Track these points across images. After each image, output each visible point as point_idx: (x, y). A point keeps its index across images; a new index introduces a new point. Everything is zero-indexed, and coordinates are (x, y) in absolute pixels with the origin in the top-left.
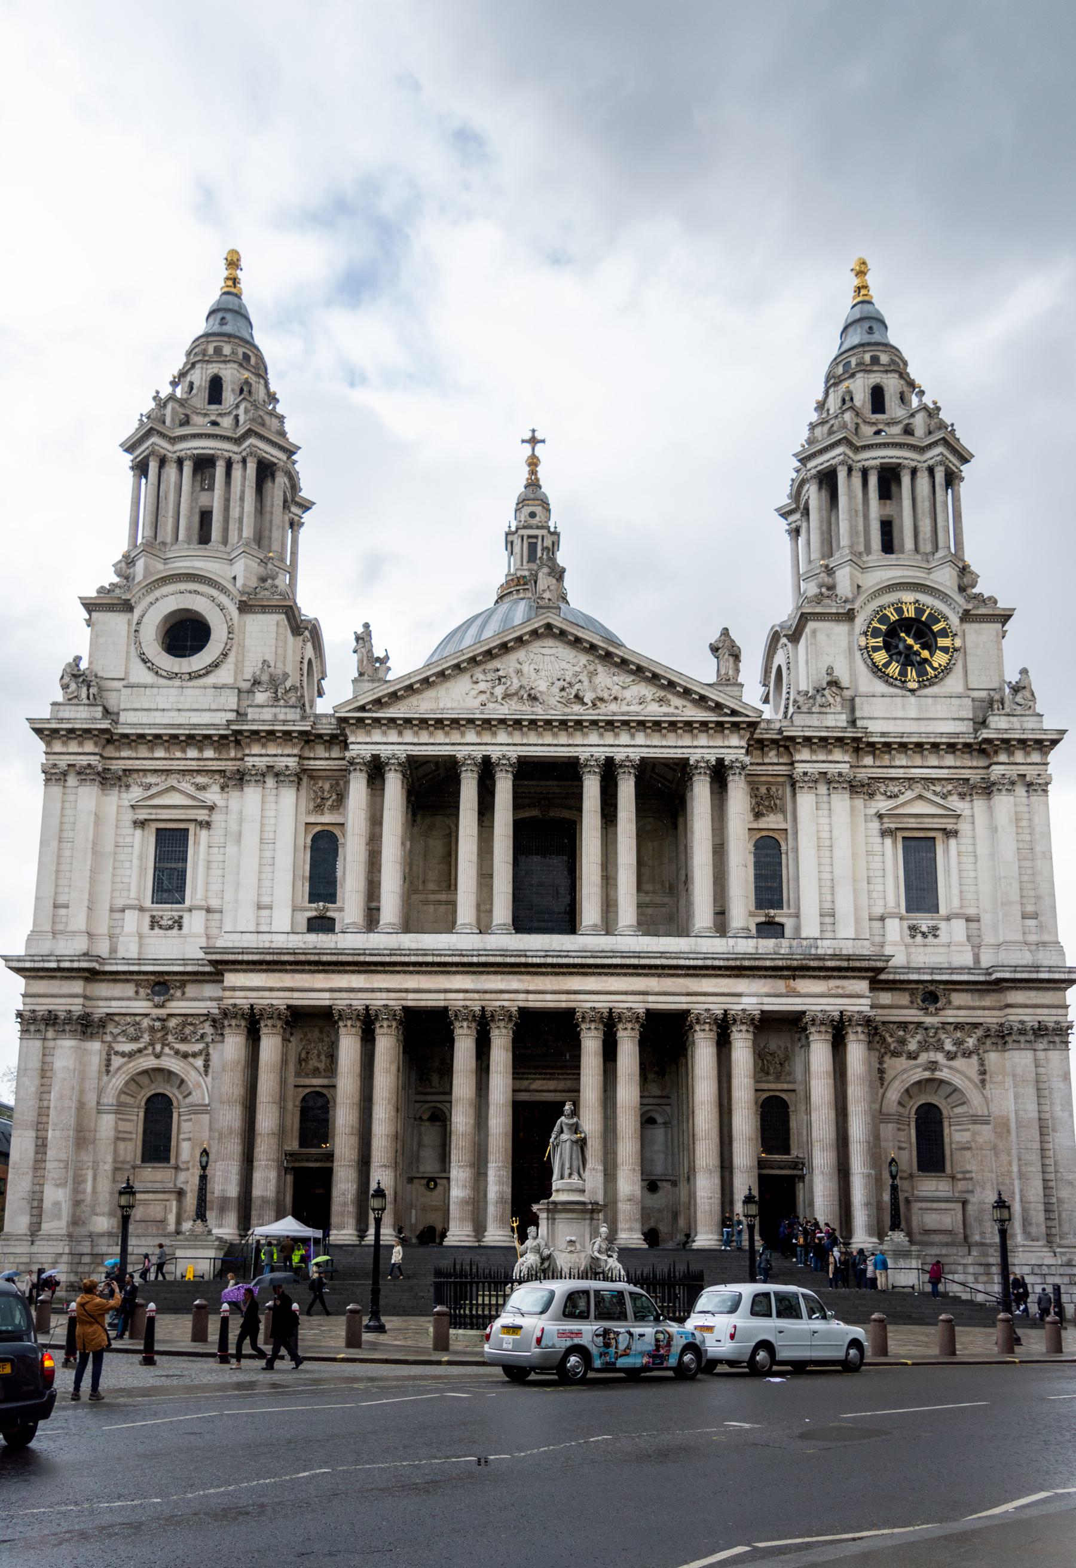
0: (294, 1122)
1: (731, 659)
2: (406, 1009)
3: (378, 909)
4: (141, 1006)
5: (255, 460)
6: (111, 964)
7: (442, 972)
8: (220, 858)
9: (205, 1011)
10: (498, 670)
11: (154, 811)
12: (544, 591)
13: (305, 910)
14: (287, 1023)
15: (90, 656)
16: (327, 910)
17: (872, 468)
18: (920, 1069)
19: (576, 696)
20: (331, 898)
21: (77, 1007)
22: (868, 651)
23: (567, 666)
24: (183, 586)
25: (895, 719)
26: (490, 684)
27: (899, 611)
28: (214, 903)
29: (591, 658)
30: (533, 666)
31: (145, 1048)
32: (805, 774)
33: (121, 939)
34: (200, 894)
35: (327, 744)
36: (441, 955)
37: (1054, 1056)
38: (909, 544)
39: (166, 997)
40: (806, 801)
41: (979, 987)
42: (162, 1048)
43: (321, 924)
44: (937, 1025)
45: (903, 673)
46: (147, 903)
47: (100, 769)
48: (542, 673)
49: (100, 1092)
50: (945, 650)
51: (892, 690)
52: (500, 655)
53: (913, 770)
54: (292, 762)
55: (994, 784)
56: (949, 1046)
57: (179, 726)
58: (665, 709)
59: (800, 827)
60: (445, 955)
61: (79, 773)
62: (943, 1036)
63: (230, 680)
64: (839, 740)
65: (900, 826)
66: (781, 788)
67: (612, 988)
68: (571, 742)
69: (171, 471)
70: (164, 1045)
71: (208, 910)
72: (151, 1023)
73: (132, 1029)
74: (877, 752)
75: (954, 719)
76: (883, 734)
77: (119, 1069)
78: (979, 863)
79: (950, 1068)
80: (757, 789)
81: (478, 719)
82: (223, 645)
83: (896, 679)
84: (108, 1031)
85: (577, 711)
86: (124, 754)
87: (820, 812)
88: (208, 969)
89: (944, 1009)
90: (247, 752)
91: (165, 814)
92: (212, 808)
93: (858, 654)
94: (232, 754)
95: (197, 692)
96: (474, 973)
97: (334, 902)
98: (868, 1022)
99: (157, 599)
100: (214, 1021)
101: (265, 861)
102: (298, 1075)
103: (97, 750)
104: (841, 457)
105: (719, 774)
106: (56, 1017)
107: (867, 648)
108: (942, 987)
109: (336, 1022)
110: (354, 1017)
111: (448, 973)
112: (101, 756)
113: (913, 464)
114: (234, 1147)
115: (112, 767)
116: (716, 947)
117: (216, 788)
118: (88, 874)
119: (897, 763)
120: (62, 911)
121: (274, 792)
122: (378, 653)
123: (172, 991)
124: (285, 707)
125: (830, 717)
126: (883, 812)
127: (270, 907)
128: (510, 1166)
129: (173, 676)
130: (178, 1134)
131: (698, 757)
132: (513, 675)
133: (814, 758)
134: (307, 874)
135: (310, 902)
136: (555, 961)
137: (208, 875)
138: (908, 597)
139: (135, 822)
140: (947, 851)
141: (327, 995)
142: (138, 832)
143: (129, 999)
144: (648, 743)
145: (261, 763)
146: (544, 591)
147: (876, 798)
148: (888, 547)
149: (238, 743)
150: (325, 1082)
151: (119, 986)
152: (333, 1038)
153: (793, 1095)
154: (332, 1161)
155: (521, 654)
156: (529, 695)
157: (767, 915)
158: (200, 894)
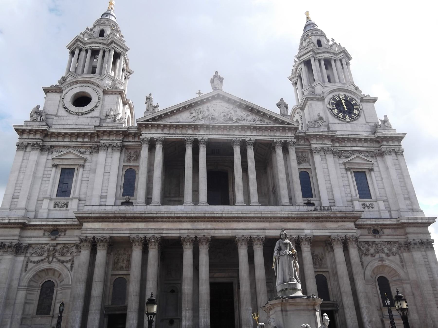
0: (110, 292)
1: (285, 108)
2: (162, 237)
3: (151, 198)
6: (34, 221)
7: (178, 222)
8: (87, 179)
9: (74, 242)
10: (200, 109)
11: (61, 161)
12: (216, 85)
17: (322, 59)
18: (377, 261)
19: (230, 118)
20: (133, 195)
21: (15, 240)
22: (331, 110)
23: (226, 109)
25: (344, 131)
28: (82, 197)
29: (235, 106)
30: (213, 108)
31: (45, 259)
32: (316, 148)
33: (40, 211)
34: (77, 193)
36: (178, 214)
37: (429, 253)
38: (337, 80)
39: (57, 236)
40: (317, 158)
41: (394, 227)
42: (53, 259)
43: (127, 203)
44: (381, 243)
46: (54, 196)
47: (41, 144)
49: (20, 280)
50: (357, 109)
51: (341, 122)
53: (354, 148)
54: (119, 143)
55: (384, 152)
56: (386, 251)
58: (262, 123)
60: (180, 214)
61: (32, 146)
62: (384, 247)
64: (326, 136)
65: (352, 167)
66: (306, 154)
68: (228, 134)
69: (83, 54)
71: (80, 200)
72: (49, 248)
74: (340, 141)
75: (365, 131)
76: (342, 135)
77: (31, 269)
79: (389, 260)
80: (298, 154)
81: (193, 125)
83: (342, 118)
84: (28, 252)
86: (52, 140)
88: (76, 223)
89: (382, 236)
90: (102, 139)
91: (66, 162)
92: (85, 160)
93: (327, 111)
95: (84, 119)
96: (192, 222)
97: (133, 196)
98: (356, 239)
99: (73, 88)
100: (77, 246)
101: (105, 180)
102: (113, 270)
103: (41, 138)
104: (311, 55)
105: (285, 147)
106: (5, 245)
107: (330, 108)
108: (380, 227)
109: (132, 244)
110: (139, 241)
111: (181, 222)
112: (42, 140)
113: (335, 58)
114: (80, 303)
116: (292, 211)
117: (88, 153)
118: (29, 184)
119: (347, 145)
120: (16, 200)
121: (111, 153)
122: (154, 104)
123: (60, 233)
127: (106, 197)
128: (209, 309)
129: (75, 114)
130: (55, 300)
131: (277, 140)
132: (206, 110)
133: (318, 143)
134: (122, 185)
135: (123, 196)
136: (226, 215)
137: (81, 186)
138: (342, 93)
139: (53, 165)
140: (371, 176)
141: (128, 232)
142: (54, 169)
143: (40, 237)
144: (258, 134)
145: (107, 143)
146: (216, 85)
147: (342, 158)
148: (329, 81)
149: (98, 136)
150: (125, 272)
152: (130, 253)
153: (327, 273)
154: (127, 310)
155: (208, 104)
156: (212, 118)
157: (307, 200)
158: (77, 193)
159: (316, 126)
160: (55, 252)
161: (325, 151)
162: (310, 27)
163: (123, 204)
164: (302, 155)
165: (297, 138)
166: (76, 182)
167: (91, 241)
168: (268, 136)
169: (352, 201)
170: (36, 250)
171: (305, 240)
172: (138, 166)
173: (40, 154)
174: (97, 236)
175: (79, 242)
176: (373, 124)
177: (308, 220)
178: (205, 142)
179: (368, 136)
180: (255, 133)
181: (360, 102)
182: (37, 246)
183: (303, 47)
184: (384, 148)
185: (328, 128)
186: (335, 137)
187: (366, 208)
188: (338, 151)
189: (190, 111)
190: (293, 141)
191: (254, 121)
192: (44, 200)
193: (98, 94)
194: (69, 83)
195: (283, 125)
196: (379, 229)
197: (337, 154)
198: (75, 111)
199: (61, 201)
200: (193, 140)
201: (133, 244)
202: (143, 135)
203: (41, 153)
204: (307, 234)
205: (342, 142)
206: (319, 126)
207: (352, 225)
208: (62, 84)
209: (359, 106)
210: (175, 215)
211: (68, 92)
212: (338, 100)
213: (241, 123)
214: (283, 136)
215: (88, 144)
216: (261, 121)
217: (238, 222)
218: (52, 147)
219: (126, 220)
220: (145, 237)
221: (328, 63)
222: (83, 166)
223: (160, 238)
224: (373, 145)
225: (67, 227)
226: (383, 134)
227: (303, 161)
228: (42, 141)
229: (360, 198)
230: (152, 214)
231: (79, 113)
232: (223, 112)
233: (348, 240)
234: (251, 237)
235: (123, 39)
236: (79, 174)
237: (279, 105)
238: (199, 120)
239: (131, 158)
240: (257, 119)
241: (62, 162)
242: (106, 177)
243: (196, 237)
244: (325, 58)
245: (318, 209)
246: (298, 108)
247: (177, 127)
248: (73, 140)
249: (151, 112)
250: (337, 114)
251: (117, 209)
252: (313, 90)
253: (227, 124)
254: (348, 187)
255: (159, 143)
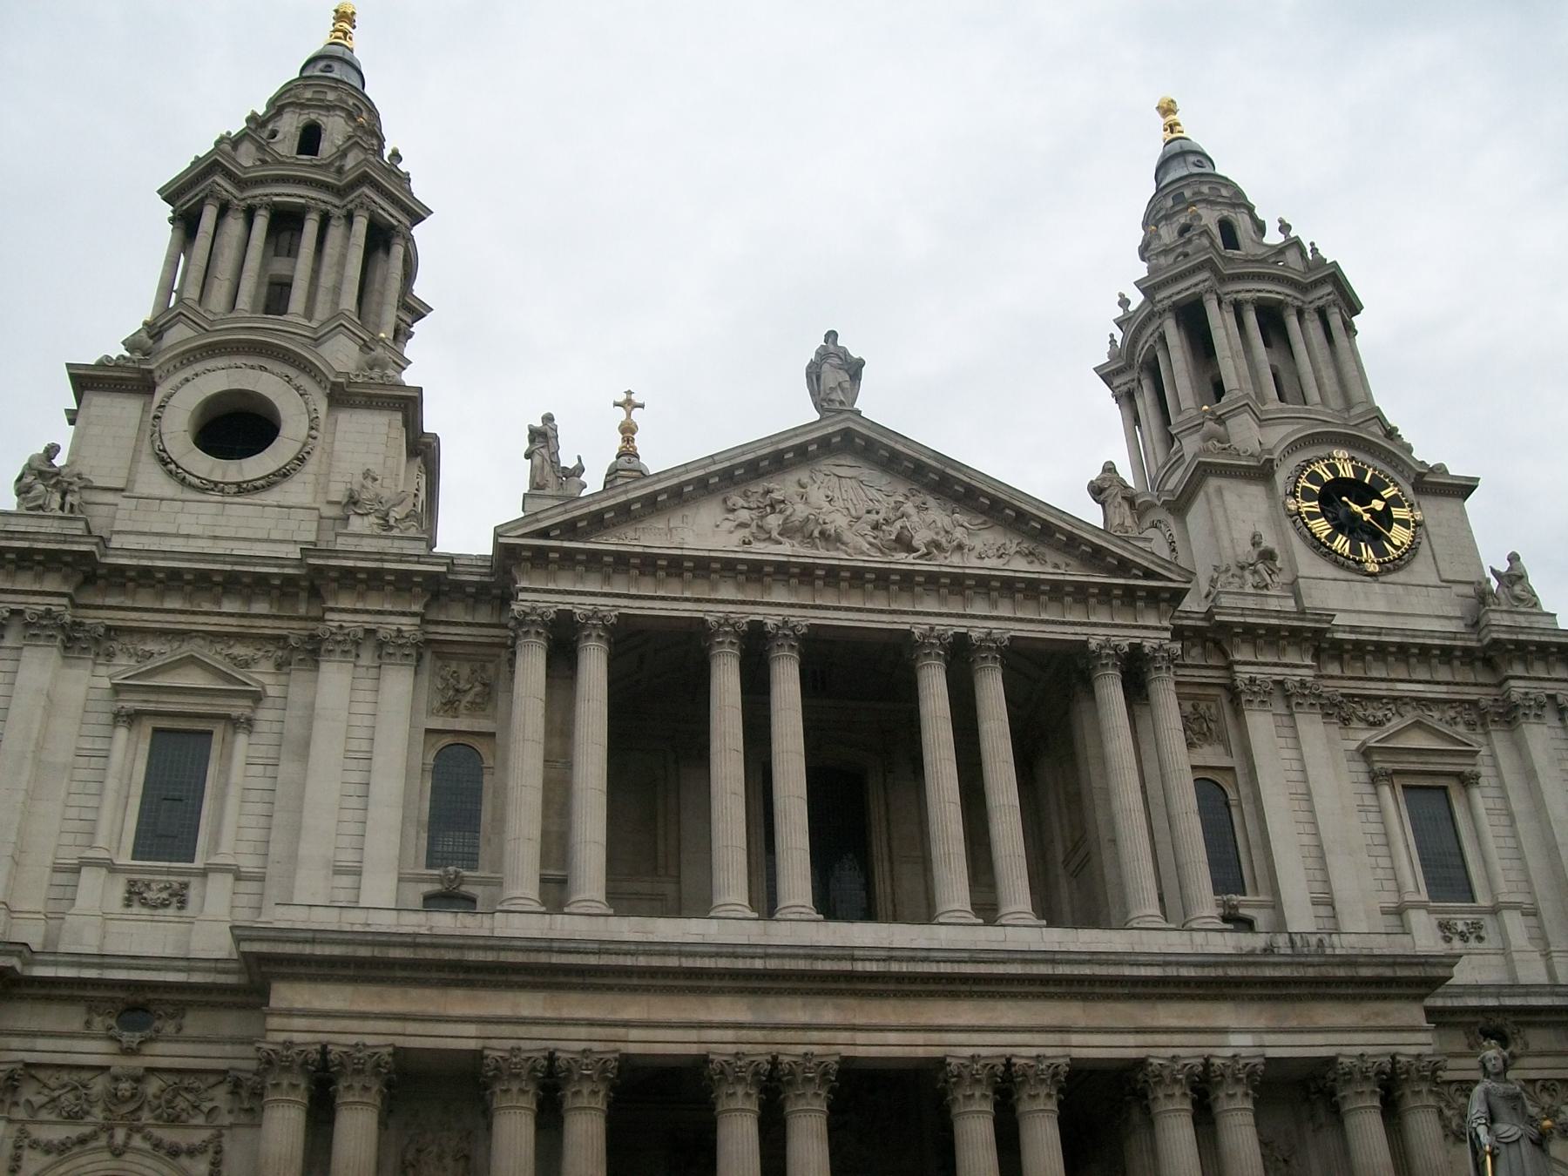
1: (1126, 506)
2: (625, 1059)
4: (93, 1051)
5: (367, 216)
6: (45, 964)
8: (267, 784)
10: (769, 492)
11: (153, 697)
13: (420, 879)
14: (389, 1085)
15: (71, 454)
16: (461, 880)
19: (899, 539)
20: (472, 861)
24: (239, 361)
25: (1359, 612)
26: (755, 514)
27: (1333, 468)
28: (248, 863)
32: (1252, 681)
35: (471, 601)
38: (1313, 395)
39: (148, 1033)
40: (1261, 725)
42: (129, 1137)
45: (1355, 550)
48: (839, 504)
50: (1404, 523)
51: (1342, 574)
52: (768, 473)
55: (1517, 706)
57: (214, 557)
58: (1036, 567)
59: (1259, 760)
60: (703, 955)
63: (307, 500)
65: (1397, 767)
67: (1005, 1022)
69: (235, 226)
70: (132, 1130)
71: (239, 876)
73: (71, 1096)
74: (1346, 657)
76: (1353, 629)
78: (1519, 825)
82: (299, 446)
85: (903, 560)
86: (110, 601)
87: (1282, 742)
90: (331, 604)
92: (257, 697)
93: (1288, 523)
94: (302, 611)
97: (474, 868)
99: (197, 375)
100: (237, 1085)
103: (65, 589)
108: (1513, 1019)
113: (1300, 304)
115: (88, 621)
117: (267, 666)
119: (1374, 674)
121: (373, 672)
124: (402, 538)
125: (1269, 599)
126: (1372, 744)
134: (425, 817)
136: (905, 968)
138: (1341, 453)
141: (471, 1029)
142: (122, 734)
143: (71, 1035)
151: (55, 1009)
155: (803, 475)
156: (822, 533)
159: (1249, 589)
160: (139, 1108)
161: (1289, 697)
162: (1183, 164)
163: (433, 902)
164: (1195, 709)
165: (1178, 633)
166: (221, 797)
167: (312, 1064)
168: (1064, 623)
169: (1399, 911)
170: (56, 1094)
171: (1234, 1075)
172: (493, 735)
173: (60, 662)
174: (337, 1044)
175: (253, 1065)
176: (1469, 590)
177: (1243, 991)
178: (797, 638)
179: (1455, 639)
180: (1004, 610)
181: (1412, 492)
182: (57, 1075)
183: (1166, 245)
184: (1517, 688)
185: (1297, 596)
186: (1328, 635)
187: (1457, 945)
188: (1340, 699)
189: (725, 501)
190: (1167, 651)
191: (1000, 557)
192: (84, 870)
193: (307, 404)
194: (184, 353)
195: (1125, 578)
196: (1508, 1031)
197: (1338, 711)
198: (211, 471)
199: (158, 877)
200: (745, 628)
201: (498, 1088)
202: (521, 596)
203: (64, 657)
204: (1237, 1050)
205: (1352, 658)
206: (1262, 588)
207: (1414, 1014)
208: (147, 353)
209: (1411, 511)
210: (683, 960)
211: (178, 388)
212: (1329, 482)
213: (947, 562)
214: (1126, 626)
215: (269, 627)
216: (1031, 558)
217: (953, 996)
218: (113, 632)
219: (461, 976)
220: (551, 1057)
221: (1272, 321)
222: (248, 724)
223: (616, 1060)
224: (1472, 676)
225: (187, 997)
226: (1512, 633)
227: (1201, 737)
228: (69, 606)
229: (1433, 898)
230: (579, 952)
231: (227, 484)
232: (869, 512)
233: (1402, 1073)
234: (1009, 1063)
235: (402, 167)
236: (230, 757)
237: (1097, 491)
238: (764, 540)
239: (460, 696)
240: (1014, 548)
241: (157, 702)
242: (356, 777)
243: (775, 1061)
244: (1259, 297)
245: (1281, 945)
246: (1159, 503)
247: (677, 567)
248: (203, 604)
249: (552, 497)
250: (1326, 537)
251: (419, 926)
252: (1222, 429)
253: (893, 566)
254: (1384, 850)
255: (594, 634)
